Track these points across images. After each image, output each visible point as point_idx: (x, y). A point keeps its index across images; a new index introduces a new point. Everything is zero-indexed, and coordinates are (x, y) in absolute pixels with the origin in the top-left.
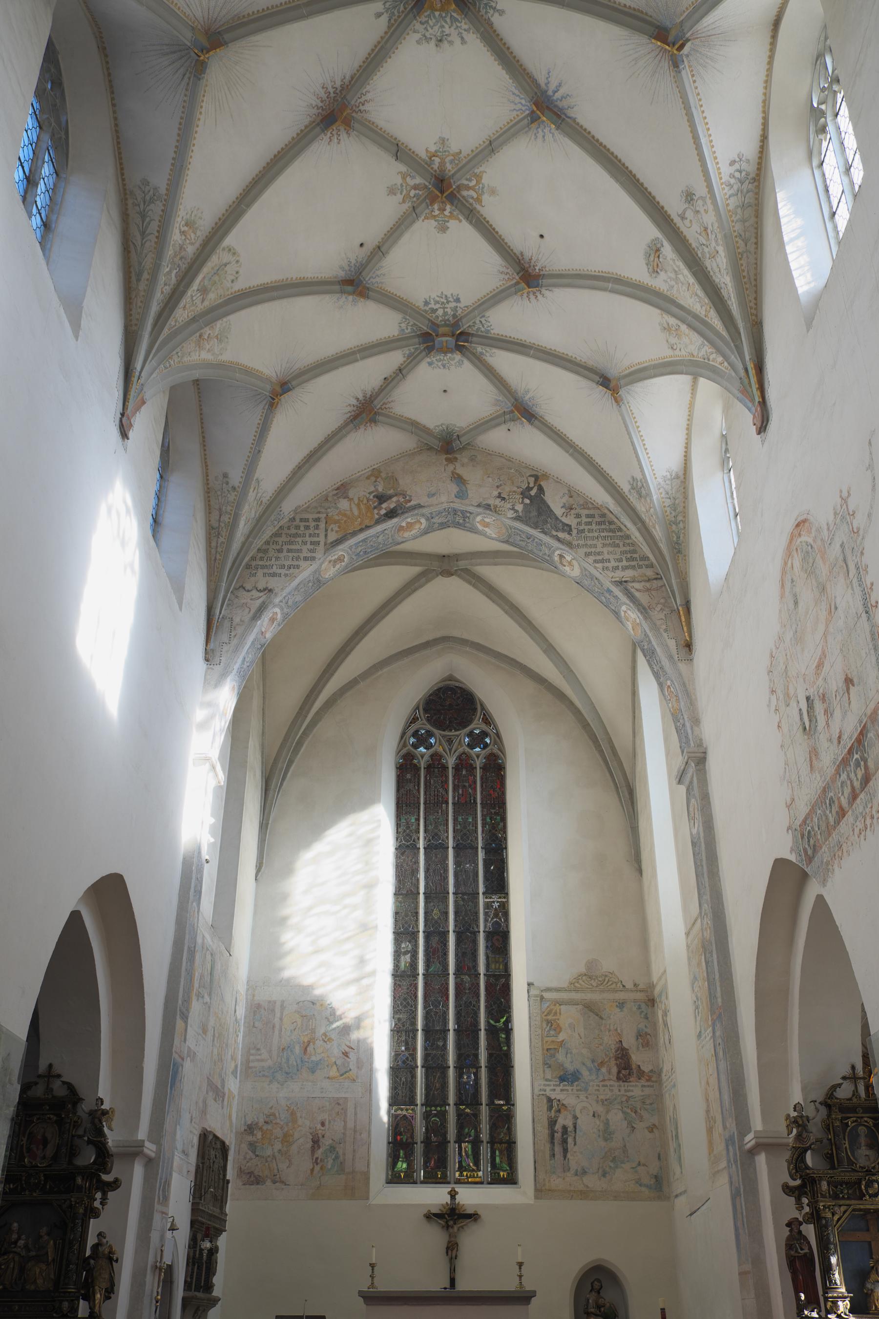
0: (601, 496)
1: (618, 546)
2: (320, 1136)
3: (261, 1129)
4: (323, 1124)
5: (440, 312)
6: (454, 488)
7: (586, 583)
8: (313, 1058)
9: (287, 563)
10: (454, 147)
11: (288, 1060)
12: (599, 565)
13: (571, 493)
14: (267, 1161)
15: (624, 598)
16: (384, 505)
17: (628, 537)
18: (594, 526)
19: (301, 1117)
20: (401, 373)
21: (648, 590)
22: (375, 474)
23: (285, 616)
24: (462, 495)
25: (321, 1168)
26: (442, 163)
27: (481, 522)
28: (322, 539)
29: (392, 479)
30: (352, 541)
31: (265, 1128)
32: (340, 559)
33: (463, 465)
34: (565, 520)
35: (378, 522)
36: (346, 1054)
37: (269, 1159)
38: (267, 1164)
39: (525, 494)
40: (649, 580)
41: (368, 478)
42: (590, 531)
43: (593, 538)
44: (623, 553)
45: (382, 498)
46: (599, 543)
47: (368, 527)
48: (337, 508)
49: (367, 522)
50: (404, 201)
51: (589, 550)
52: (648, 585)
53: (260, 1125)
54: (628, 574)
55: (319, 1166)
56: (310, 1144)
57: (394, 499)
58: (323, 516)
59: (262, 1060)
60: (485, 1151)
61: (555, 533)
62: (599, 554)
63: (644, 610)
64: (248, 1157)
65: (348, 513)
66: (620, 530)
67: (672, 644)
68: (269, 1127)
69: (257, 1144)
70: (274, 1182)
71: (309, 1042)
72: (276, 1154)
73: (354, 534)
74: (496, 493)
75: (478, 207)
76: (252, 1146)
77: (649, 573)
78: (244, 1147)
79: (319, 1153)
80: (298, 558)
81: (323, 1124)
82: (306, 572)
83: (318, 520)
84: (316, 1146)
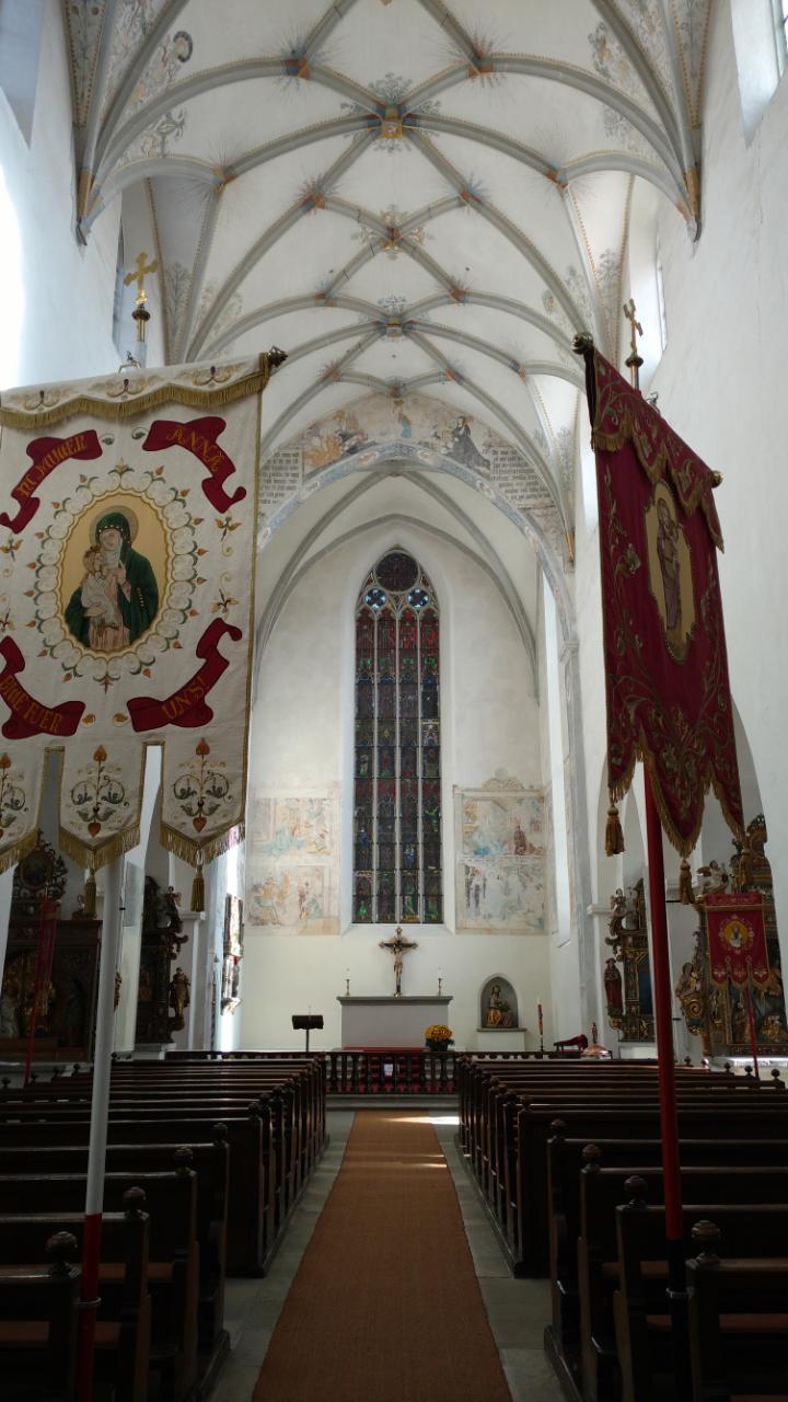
0: (512, 439)
1: (525, 479)
3: (263, 888)
4: (307, 884)
5: (391, 308)
6: (400, 428)
7: (501, 505)
9: (274, 492)
10: (402, 210)
11: (281, 840)
12: (510, 495)
13: (491, 433)
15: (527, 522)
16: (347, 443)
17: (532, 471)
18: (507, 462)
20: (360, 347)
21: (545, 516)
22: (340, 415)
23: (274, 531)
24: (406, 434)
26: (393, 217)
27: (422, 454)
28: (300, 471)
29: (353, 420)
30: (323, 473)
32: (315, 485)
33: (408, 408)
34: (486, 457)
35: (343, 457)
36: (322, 836)
39: (455, 433)
40: (547, 507)
41: (334, 418)
42: (504, 466)
43: (504, 472)
44: (529, 484)
45: (345, 437)
46: (510, 476)
47: (335, 462)
48: (311, 445)
49: (334, 458)
50: (364, 242)
51: (502, 482)
52: (545, 512)
54: (532, 502)
56: (298, 898)
57: (355, 437)
58: (300, 451)
60: (421, 901)
61: (477, 467)
62: (508, 485)
63: (541, 532)
65: (320, 450)
66: (526, 465)
67: (560, 559)
73: (324, 467)
74: (432, 433)
75: (420, 245)
77: (547, 501)
78: (252, 900)
79: (305, 904)
80: (282, 488)
81: (307, 884)
82: (289, 498)
83: (296, 455)
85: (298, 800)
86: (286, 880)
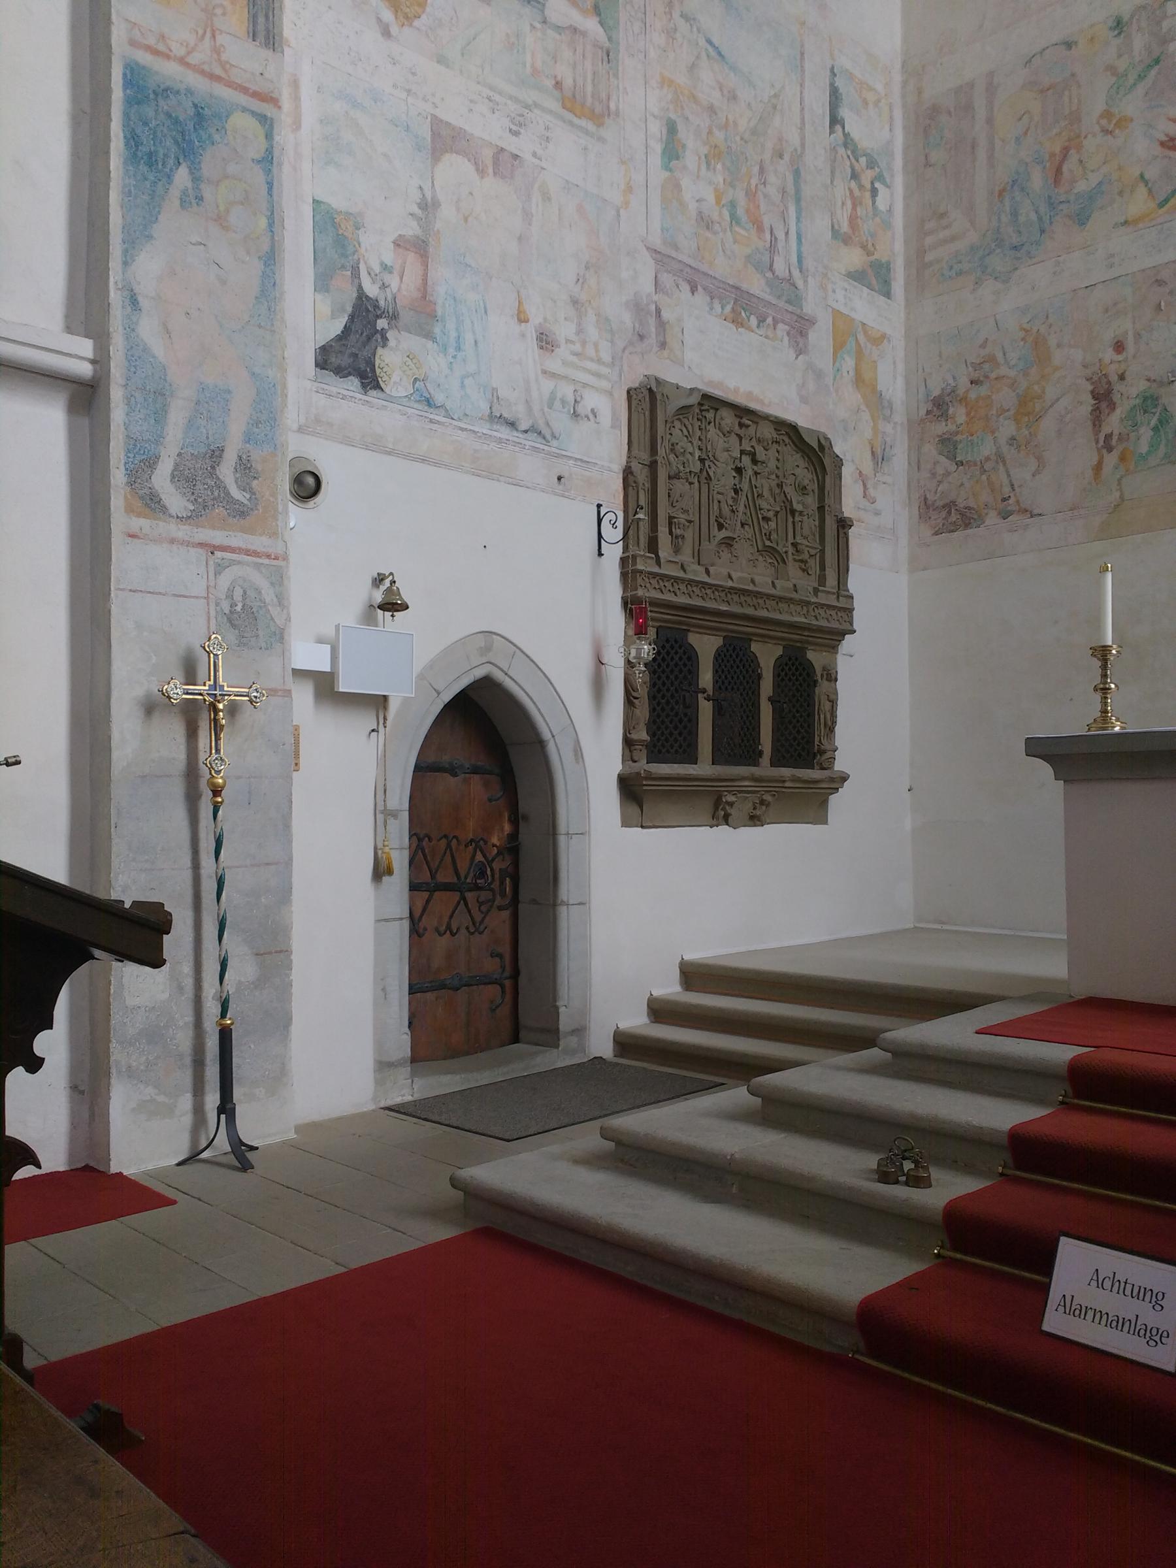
2: (1114, 378)
3: (963, 400)
4: (1119, 347)
8: (1082, 186)
11: (1015, 214)
14: (985, 471)
19: (1059, 346)
25: (1122, 458)
31: (973, 395)
37: (987, 466)
38: (984, 477)
53: (961, 391)
55: (1115, 454)
59: (953, 239)
64: (940, 470)
68: (983, 390)
69: (959, 438)
70: (1005, 515)
71: (1066, 151)
72: (1005, 449)
76: (948, 445)
78: (930, 450)
79: (1114, 423)
81: (1119, 347)
84: (1104, 405)
85: (1069, 45)
86: (1038, 347)
